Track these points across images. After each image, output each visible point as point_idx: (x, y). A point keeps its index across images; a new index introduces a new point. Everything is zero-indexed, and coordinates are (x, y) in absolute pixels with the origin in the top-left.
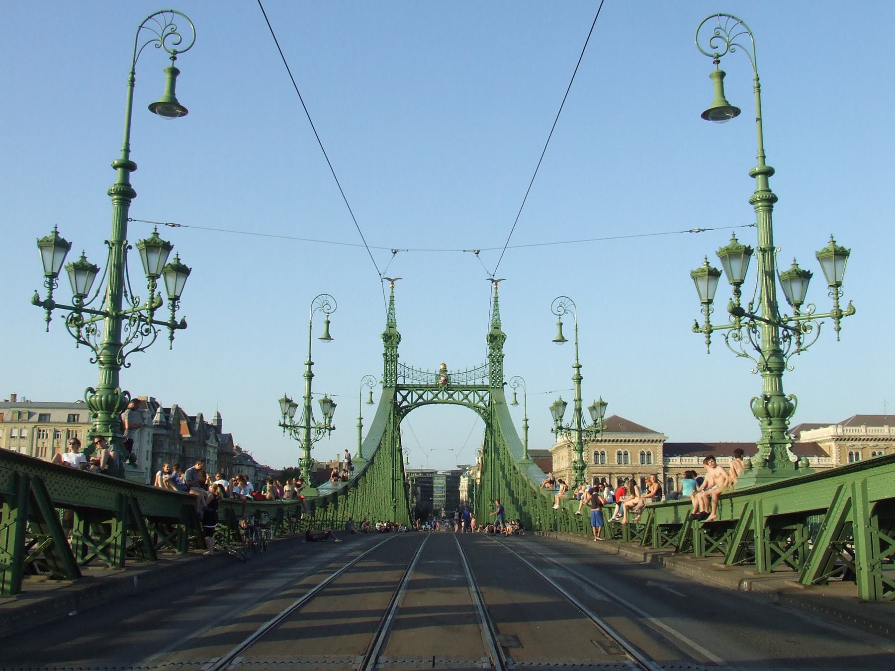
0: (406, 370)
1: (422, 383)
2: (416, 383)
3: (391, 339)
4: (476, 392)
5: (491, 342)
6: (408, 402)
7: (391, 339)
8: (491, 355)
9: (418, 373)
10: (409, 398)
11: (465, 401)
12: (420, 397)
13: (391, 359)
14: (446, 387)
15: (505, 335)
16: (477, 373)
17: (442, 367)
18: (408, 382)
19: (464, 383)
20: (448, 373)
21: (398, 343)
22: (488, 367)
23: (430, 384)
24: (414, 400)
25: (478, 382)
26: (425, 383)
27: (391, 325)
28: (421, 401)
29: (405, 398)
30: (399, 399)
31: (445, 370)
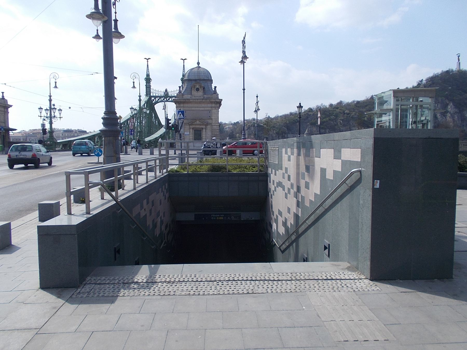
0: (154, 91)
1: (159, 95)
2: (157, 95)
3: (148, 80)
7: (148, 80)
9: (158, 92)
12: (159, 100)
13: (148, 87)
18: (154, 95)
19: (173, 95)
20: (168, 91)
23: (162, 95)
24: (157, 100)
26: (160, 95)
27: (148, 75)
28: (159, 101)
29: (153, 100)
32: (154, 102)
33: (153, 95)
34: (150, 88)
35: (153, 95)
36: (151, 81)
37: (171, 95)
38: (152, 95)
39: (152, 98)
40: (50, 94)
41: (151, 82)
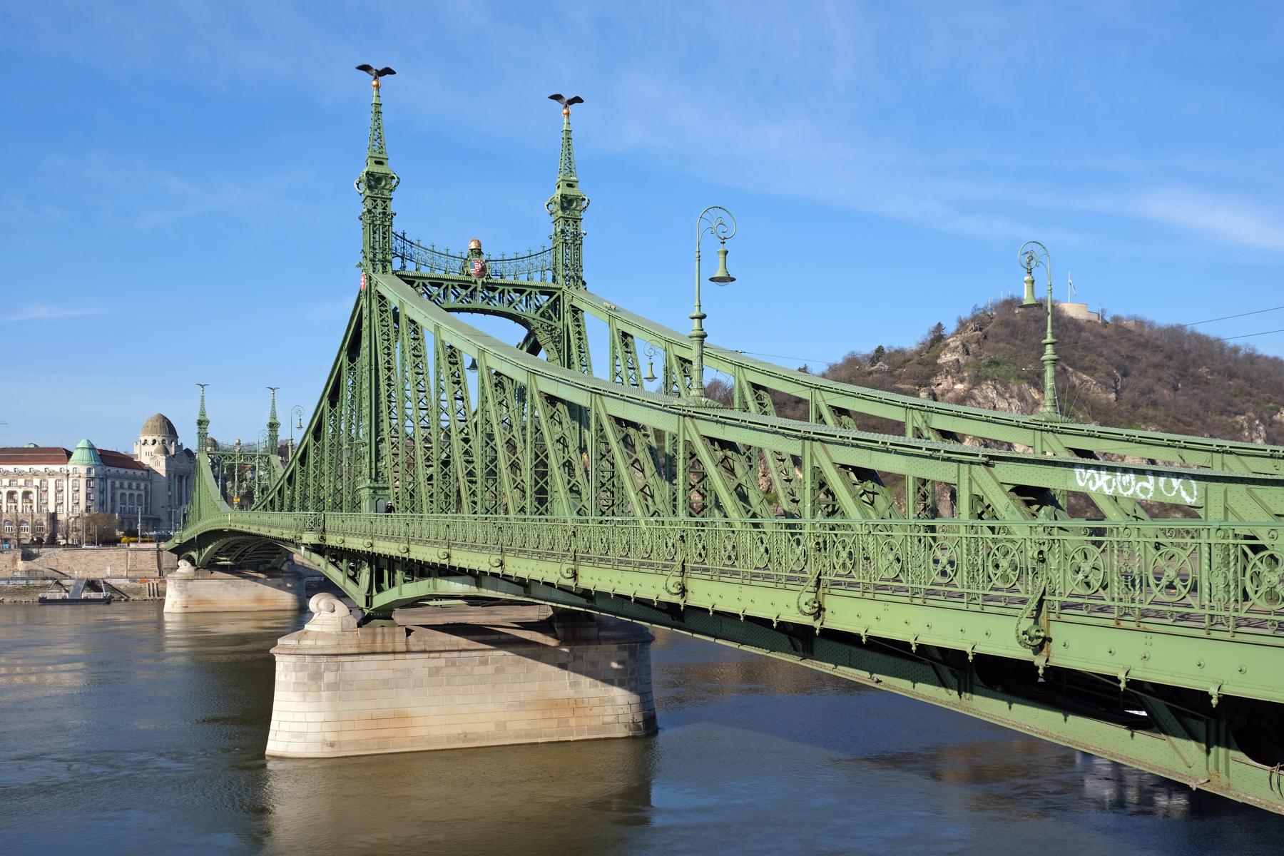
2: (425, 271)
9: (430, 255)
16: (536, 262)
17: (473, 245)
25: (536, 281)
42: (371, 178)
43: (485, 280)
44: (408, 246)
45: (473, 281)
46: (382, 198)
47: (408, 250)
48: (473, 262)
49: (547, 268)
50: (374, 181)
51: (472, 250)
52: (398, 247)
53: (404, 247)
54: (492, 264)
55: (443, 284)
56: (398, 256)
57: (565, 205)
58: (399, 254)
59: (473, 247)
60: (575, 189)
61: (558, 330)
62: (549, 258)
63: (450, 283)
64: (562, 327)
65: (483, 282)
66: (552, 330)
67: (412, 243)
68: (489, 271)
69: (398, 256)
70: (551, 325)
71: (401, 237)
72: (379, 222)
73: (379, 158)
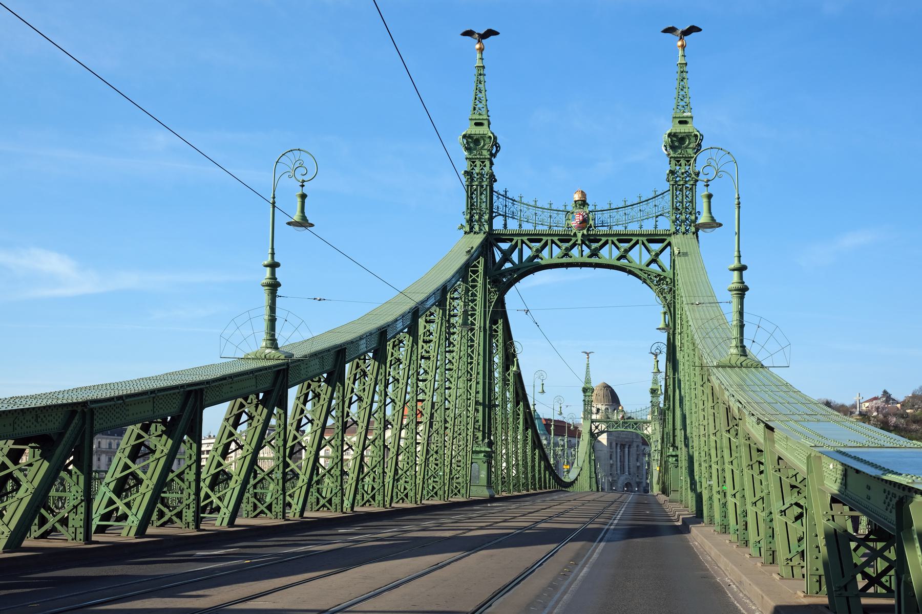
2: (527, 227)
4: (643, 244)
5: (673, 148)
6: (513, 263)
8: (672, 172)
9: (532, 211)
10: (515, 256)
11: (624, 262)
14: (585, 232)
15: (701, 135)
16: (649, 208)
17: (577, 197)
18: (513, 225)
21: (494, 155)
22: (668, 197)
23: (555, 228)
26: (546, 228)
29: (506, 256)
30: (498, 256)
31: (583, 203)
32: (508, 265)
33: (505, 225)
34: (492, 191)
35: (505, 225)
36: (494, 152)
37: (610, 227)
38: (498, 224)
39: (500, 244)
40: (273, 254)
41: (494, 160)
42: (470, 140)
43: (585, 232)
44: (510, 204)
45: (572, 234)
46: (480, 158)
47: (512, 208)
48: (575, 214)
49: (659, 213)
50: (472, 142)
51: (576, 201)
52: (500, 206)
53: (506, 206)
54: (598, 215)
55: (542, 239)
56: (500, 215)
57: (676, 144)
58: (502, 213)
59: (577, 199)
60: (688, 125)
61: (668, 280)
62: (666, 202)
63: (549, 238)
64: (672, 277)
65: (583, 235)
66: (660, 280)
67: (514, 201)
68: (591, 222)
69: (500, 215)
70: (659, 275)
71: (503, 196)
72: (476, 183)
73: (479, 119)
